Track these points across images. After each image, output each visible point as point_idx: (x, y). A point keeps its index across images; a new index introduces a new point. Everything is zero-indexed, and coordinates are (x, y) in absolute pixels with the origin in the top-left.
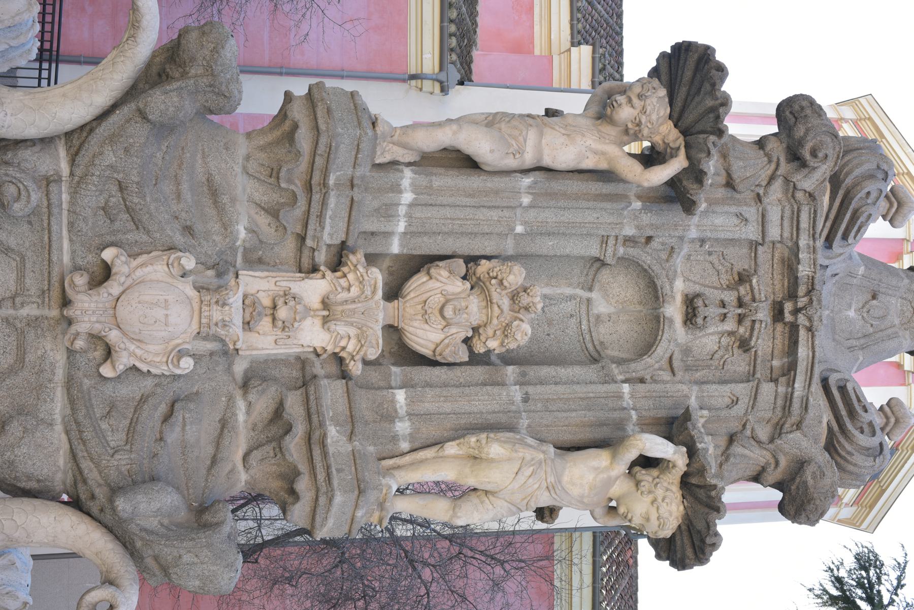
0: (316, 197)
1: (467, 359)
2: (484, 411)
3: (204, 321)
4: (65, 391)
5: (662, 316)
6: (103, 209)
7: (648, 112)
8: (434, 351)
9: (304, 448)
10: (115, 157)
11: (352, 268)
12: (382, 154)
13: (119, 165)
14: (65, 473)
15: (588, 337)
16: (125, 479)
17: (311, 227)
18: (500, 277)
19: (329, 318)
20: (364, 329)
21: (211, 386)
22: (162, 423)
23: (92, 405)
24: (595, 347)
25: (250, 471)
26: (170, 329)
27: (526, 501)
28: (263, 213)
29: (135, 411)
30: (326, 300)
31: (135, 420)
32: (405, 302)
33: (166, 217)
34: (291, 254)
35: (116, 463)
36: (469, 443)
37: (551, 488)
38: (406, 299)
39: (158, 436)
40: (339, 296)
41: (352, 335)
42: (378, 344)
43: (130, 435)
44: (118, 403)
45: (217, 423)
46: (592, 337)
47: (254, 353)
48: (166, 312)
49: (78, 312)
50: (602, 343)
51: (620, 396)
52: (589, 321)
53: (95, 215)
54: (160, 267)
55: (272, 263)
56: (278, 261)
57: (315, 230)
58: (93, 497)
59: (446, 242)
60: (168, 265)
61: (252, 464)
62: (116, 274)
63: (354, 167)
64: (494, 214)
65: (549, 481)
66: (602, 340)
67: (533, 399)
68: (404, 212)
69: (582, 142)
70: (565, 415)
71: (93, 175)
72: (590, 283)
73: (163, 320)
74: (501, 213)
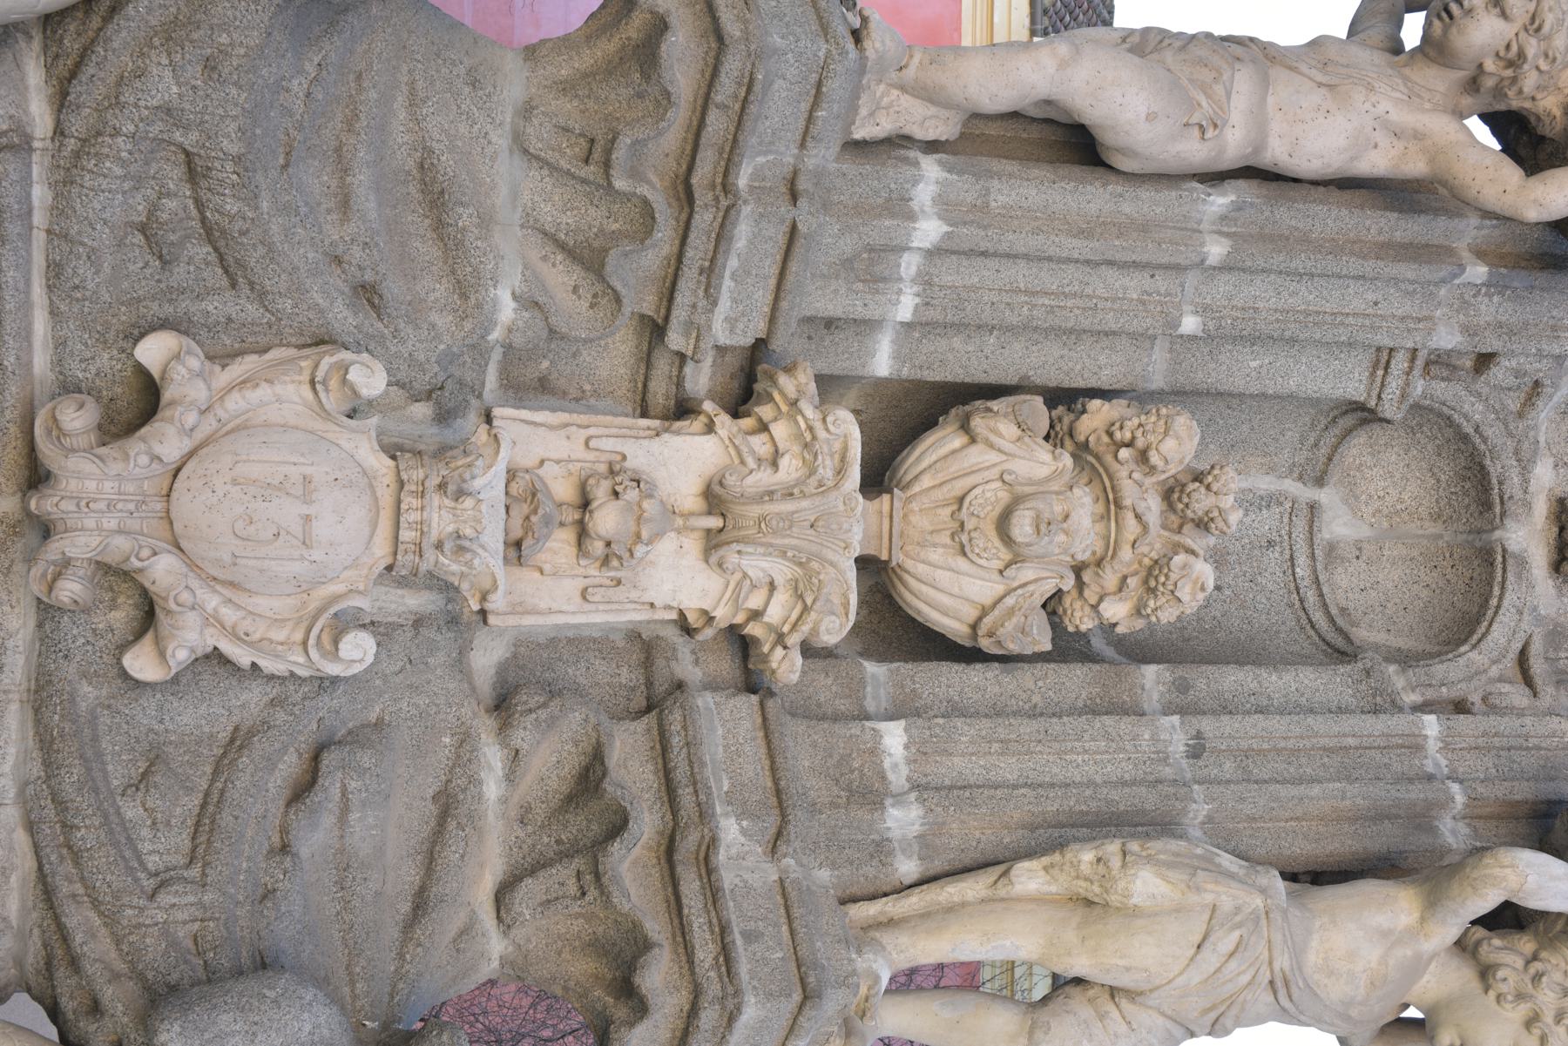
0: (704, 219)
1: (1048, 647)
2: (1098, 779)
3: (407, 535)
4: (30, 714)
5: (1499, 550)
6: (143, 229)
7: (1546, 29)
8: (974, 627)
9: (655, 873)
10: (179, 85)
11: (784, 408)
12: (872, 114)
13: (188, 106)
14: (22, 936)
15: (1311, 597)
16: (186, 962)
17: (683, 298)
18: (1140, 443)
19: (723, 537)
20: (815, 565)
21: (417, 706)
22: (288, 804)
23: (99, 755)
24: (1332, 620)
25: (514, 931)
26: (317, 555)
27: (1213, 1015)
28: (560, 257)
29: (216, 772)
30: (717, 489)
31: (215, 797)
32: (909, 500)
33: (310, 255)
34: (622, 371)
35: (161, 917)
36: (1075, 865)
37: (1279, 984)
38: (909, 493)
39: (276, 839)
40: (750, 480)
41: (779, 580)
42: (846, 605)
43: (203, 838)
44: (170, 749)
45: (429, 803)
46: (1321, 595)
47: (529, 621)
48: (305, 510)
49: (68, 506)
50: (1343, 610)
51: (1415, 746)
52: (1313, 556)
53: (120, 244)
54: (291, 387)
55: (574, 393)
56: (587, 387)
57: (694, 306)
58: (95, 1008)
59: (1006, 352)
60: (313, 383)
61: (521, 914)
62: (172, 403)
63: (803, 145)
64: (1132, 285)
65: (1277, 966)
66: (1343, 603)
67: (1214, 750)
68: (913, 270)
69: (1368, 106)
70: (1295, 791)
71: (116, 132)
72: (1320, 466)
73: (296, 528)
74: (1147, 283)
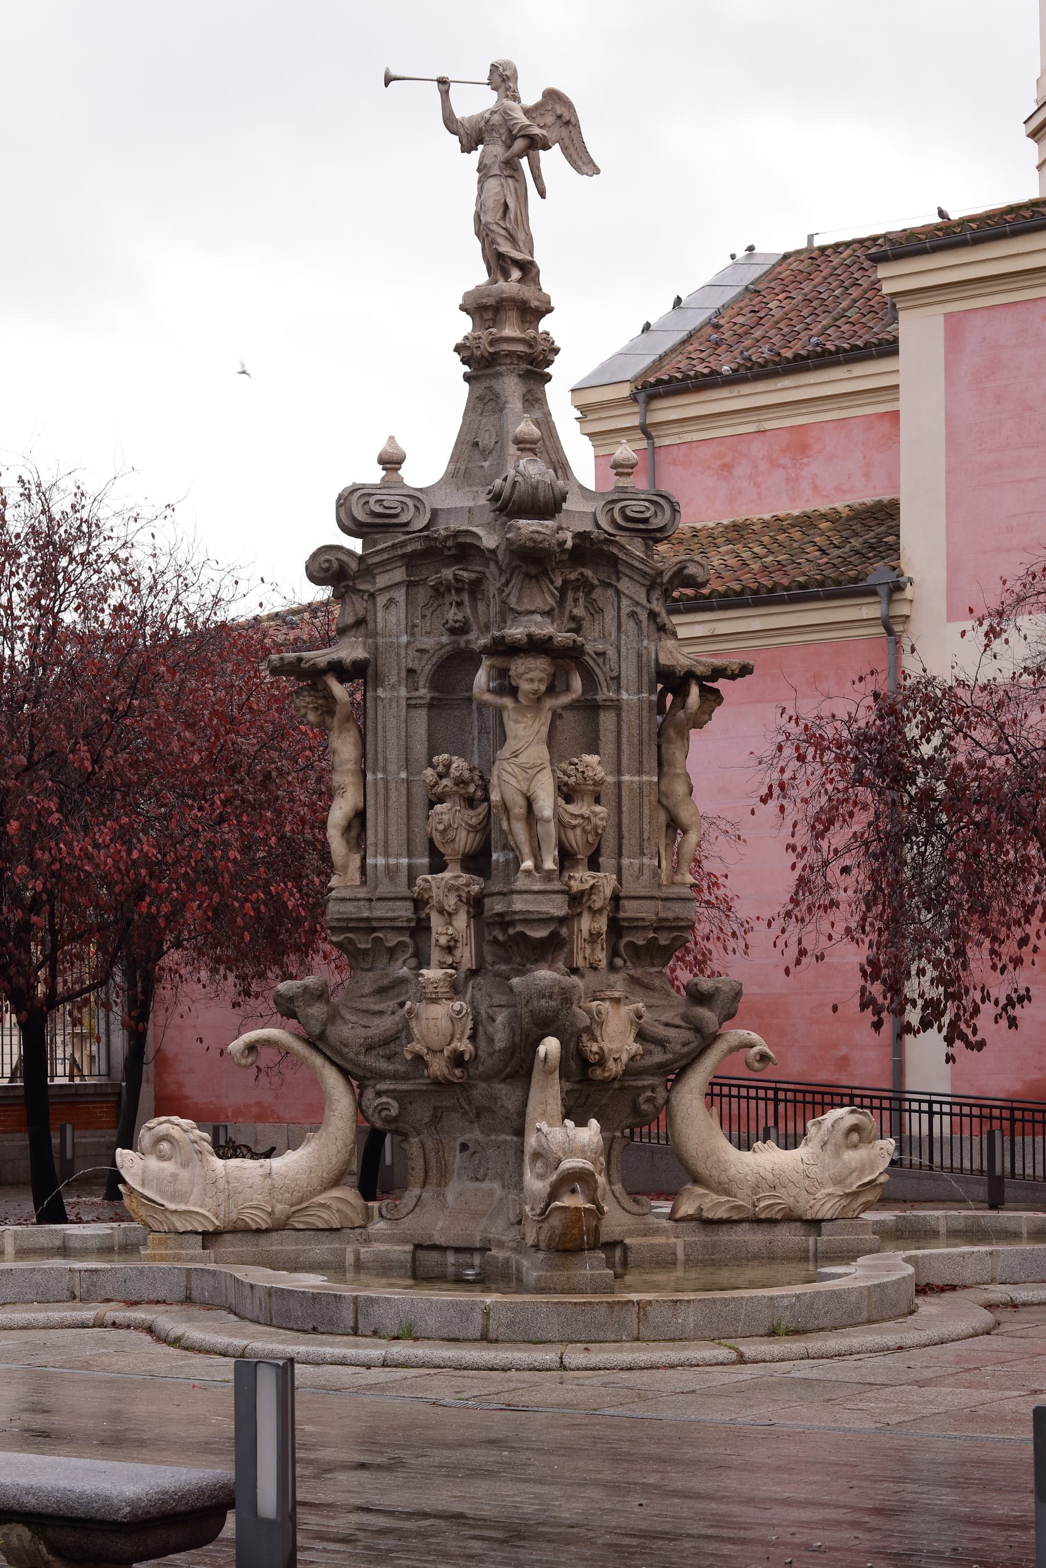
0: (375, 924)
17: (400, 924)
64: (393, 794)
